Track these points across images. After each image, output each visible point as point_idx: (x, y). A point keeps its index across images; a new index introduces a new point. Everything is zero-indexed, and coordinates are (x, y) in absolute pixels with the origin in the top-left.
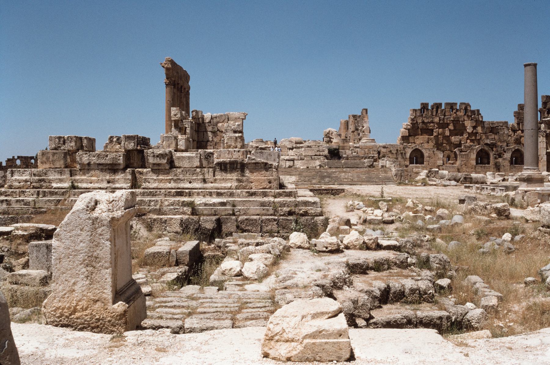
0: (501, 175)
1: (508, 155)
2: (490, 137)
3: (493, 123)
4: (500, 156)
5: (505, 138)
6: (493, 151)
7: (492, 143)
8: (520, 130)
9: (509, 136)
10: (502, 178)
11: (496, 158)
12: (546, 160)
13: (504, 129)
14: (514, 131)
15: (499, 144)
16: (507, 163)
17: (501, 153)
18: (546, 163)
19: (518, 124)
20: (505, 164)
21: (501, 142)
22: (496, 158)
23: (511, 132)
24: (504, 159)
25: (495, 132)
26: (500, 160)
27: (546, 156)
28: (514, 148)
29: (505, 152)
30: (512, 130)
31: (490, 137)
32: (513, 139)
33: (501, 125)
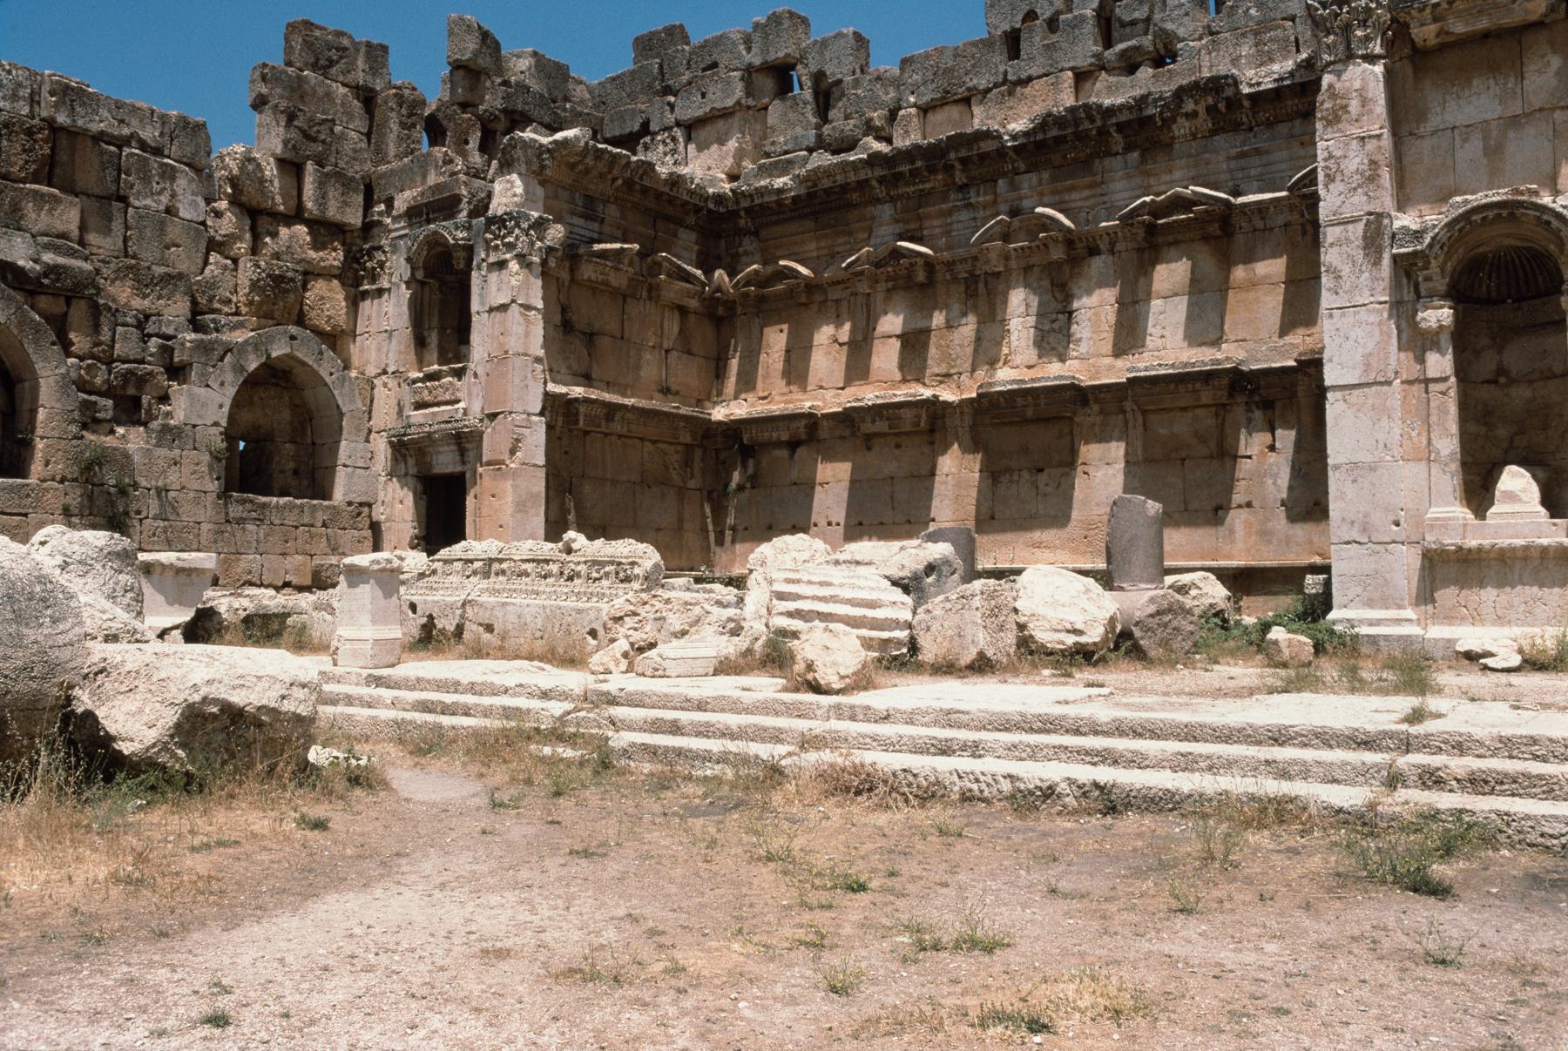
0: (181, 581)
1: (203, 404)
2: (37, 218)
3: (68, 94)
4: (131, 411)
5: (183, 260)
6: (66, 347)
7: (53, 270)
8: (296, 215)
9: (213, 245)
10: (186, 616)
11: (90, 421)
12: (541, 461)
13: (169, 174)
14: (259, 218)
15: (122, 293)
16: (195, 477)
17: (142, 381)
18: (539, 485)
19: (291, 167)
20: (173, 478)
21: (144, 283)
22: (90, 421)
23: (228, 223)
24: (171, 435)
25: (88, 177)
26: (132, 440)
27: (540, 425)
28: (256, 345)
29: (177, 372)
30: (235, 201)
31: (37, 218)
32: (247, 272)
33: (149, 134)
